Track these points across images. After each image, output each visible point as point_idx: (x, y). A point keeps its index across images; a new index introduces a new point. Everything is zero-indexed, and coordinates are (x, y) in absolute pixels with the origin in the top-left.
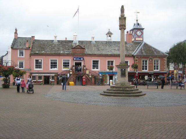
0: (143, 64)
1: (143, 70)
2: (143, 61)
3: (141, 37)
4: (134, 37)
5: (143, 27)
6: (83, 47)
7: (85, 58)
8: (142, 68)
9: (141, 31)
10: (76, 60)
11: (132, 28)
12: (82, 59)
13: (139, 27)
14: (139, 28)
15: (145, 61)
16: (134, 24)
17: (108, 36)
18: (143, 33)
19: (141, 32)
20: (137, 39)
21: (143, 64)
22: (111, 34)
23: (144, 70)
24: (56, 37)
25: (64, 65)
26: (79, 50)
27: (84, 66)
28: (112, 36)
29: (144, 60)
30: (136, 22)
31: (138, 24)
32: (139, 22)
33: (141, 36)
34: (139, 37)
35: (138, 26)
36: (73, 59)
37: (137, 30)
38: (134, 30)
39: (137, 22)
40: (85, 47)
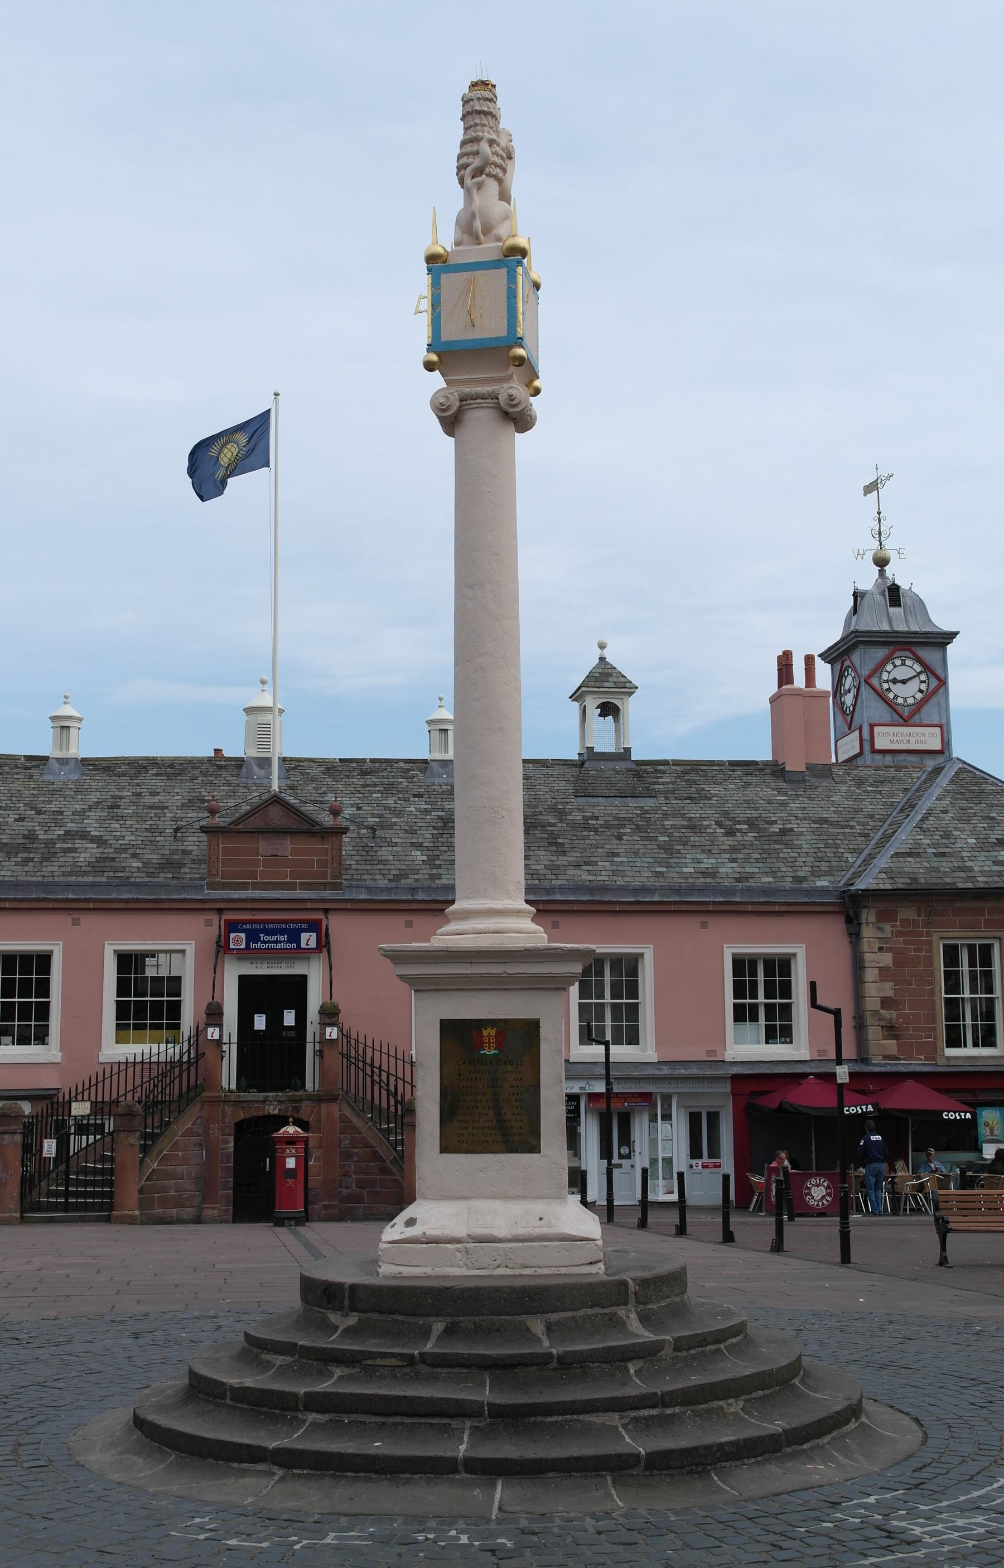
0: (953, 982)
1: (951, 1052)
2: (951, 954)
3: (930, 712)
4: (856, 723)
5: (942, 622)
6: (326, 819)
7: (337, 925)
8: (942, 1023)
9: (924, 653)
10: (242, 955)
11: (834, 634)
12: (308, 939)
13: (899, 621)
14: (902, 627)
15: (971, 948)
16: (857, 595)
17: (592, 704)
18: (943, 682)
19: (927, 668)
20: (886, 738)
21: (953, 982)
22: (627, 688)
23: (969, 1051)
24: (63, 726)
25: (122, 1011)
26: (287, 847)
27: (330, 1014)
28: (632, 707)
29: (963, 938)
30: (868, 579)
31: (894, 594)
32: (897, 573)
33: (920, 705)
34: (906, 721)
35: (894, 611)
36: (222, 947)
37: (880, 653)
38: (856, 657)
39: (882, 573)
40: (341, 822)
